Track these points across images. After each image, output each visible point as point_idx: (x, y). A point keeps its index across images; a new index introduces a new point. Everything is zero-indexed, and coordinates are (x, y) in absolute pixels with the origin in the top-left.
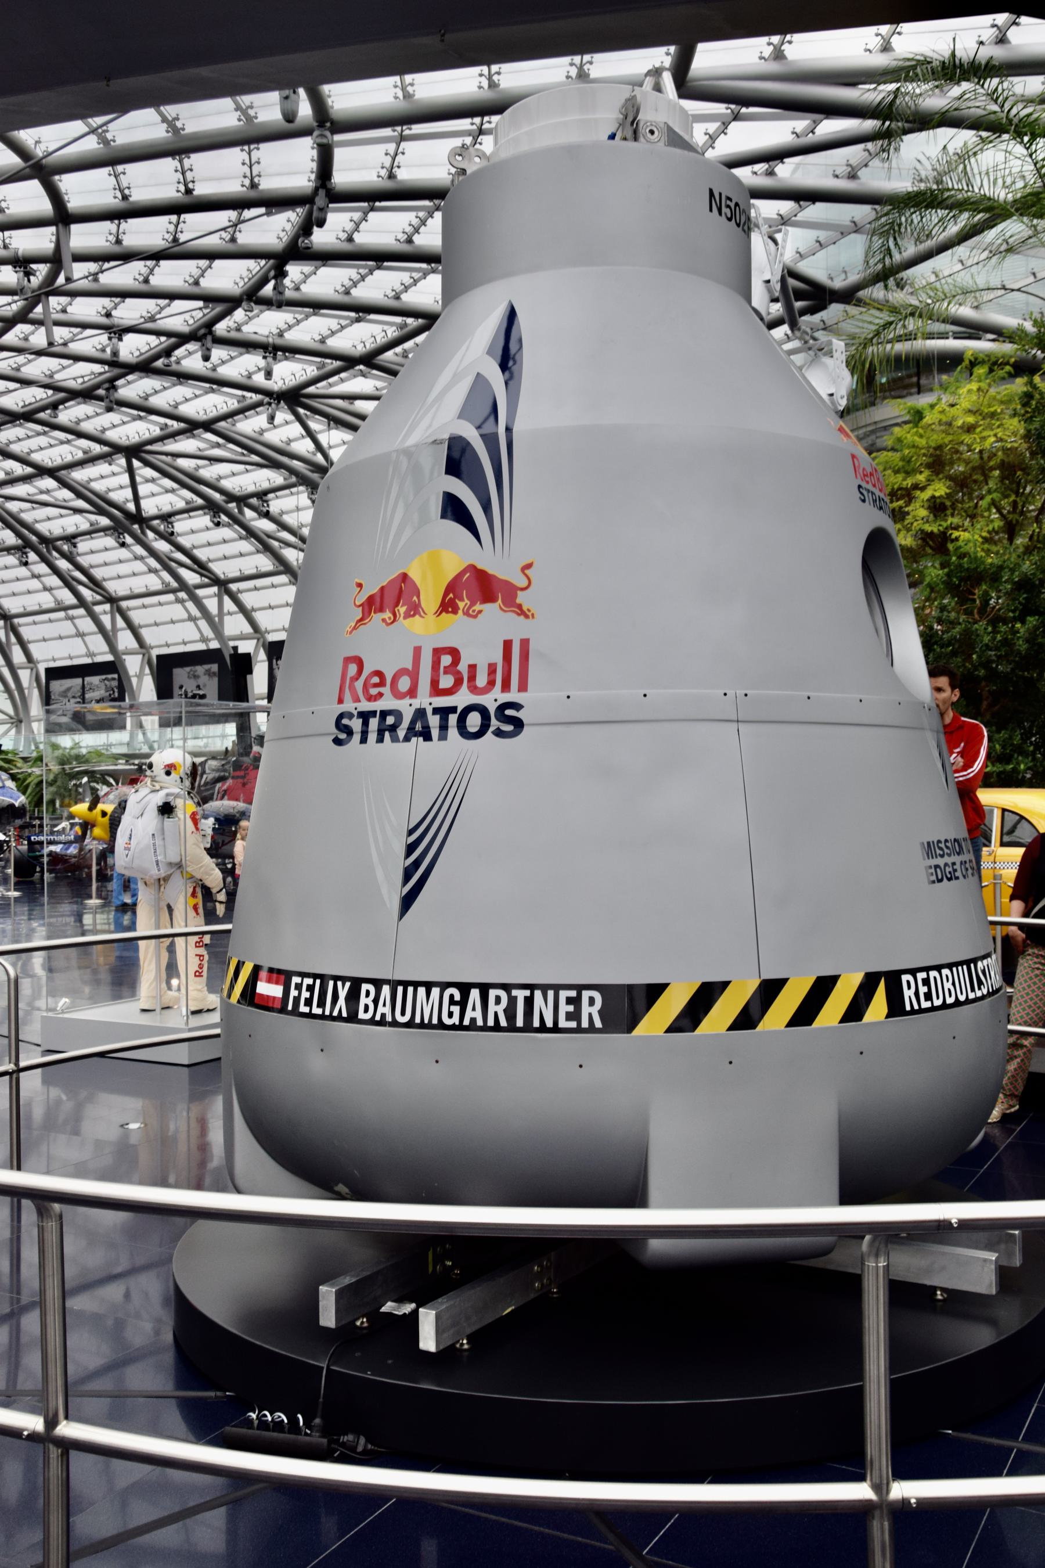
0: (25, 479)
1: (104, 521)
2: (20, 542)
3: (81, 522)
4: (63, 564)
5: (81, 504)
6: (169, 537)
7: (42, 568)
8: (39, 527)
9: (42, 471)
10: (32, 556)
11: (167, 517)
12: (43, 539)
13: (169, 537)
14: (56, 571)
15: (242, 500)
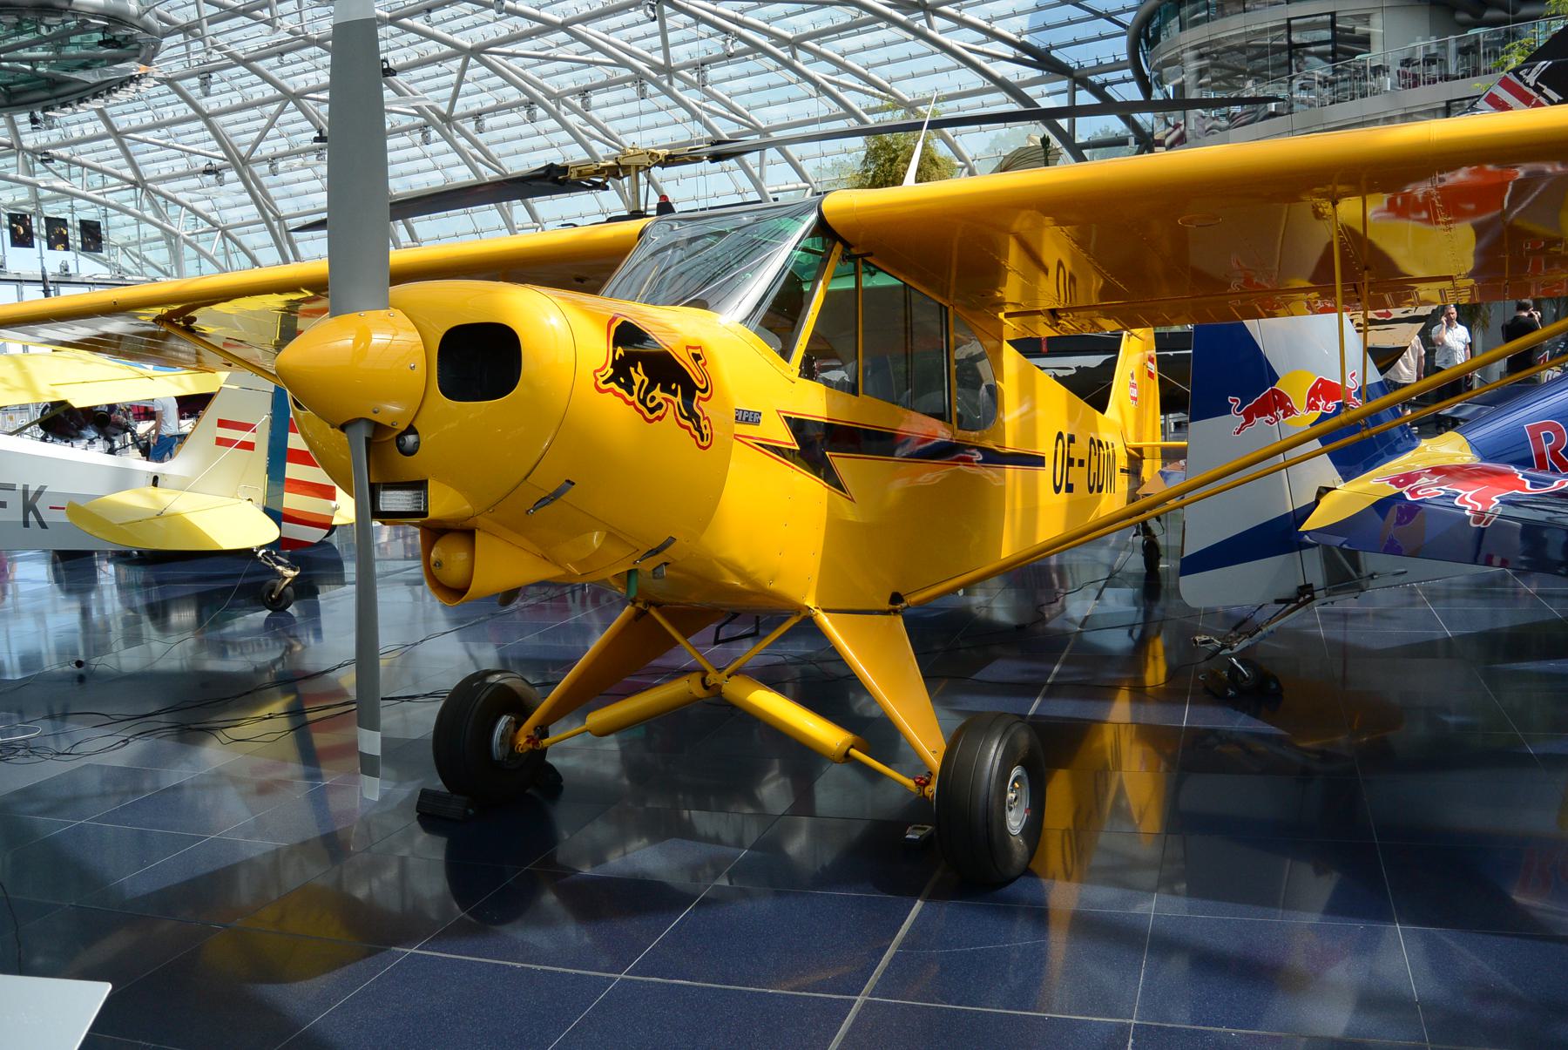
0: (527, 36)
1: (627, 72)
2: (525, 97)
3: (598, 75)
4: (573, 120)
5: (598, 57)
6: (702, 85)
7: (552, 123)
8: (545, 82)
9: (551, 27)
10: (540, 112)
11: (700, 66)
12: (550, 95)
13: (702, 85)
14: (565, 126)
15: (795, 44)
